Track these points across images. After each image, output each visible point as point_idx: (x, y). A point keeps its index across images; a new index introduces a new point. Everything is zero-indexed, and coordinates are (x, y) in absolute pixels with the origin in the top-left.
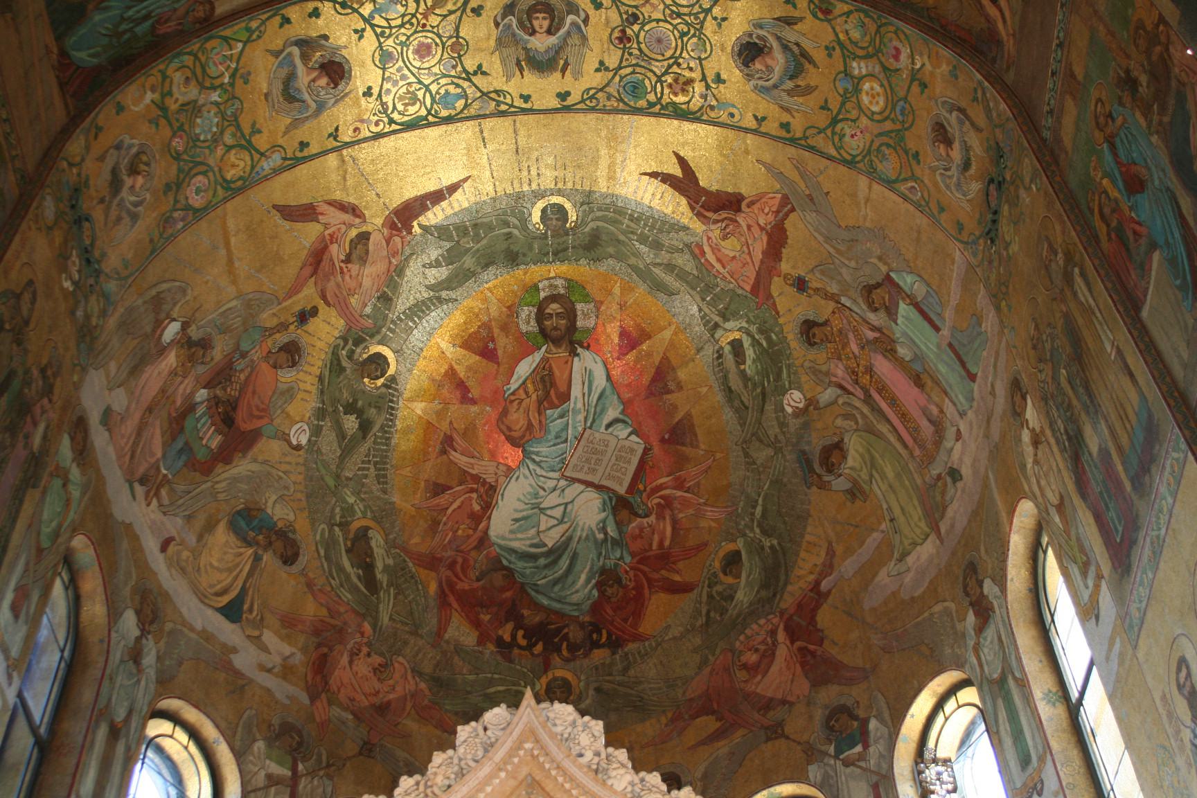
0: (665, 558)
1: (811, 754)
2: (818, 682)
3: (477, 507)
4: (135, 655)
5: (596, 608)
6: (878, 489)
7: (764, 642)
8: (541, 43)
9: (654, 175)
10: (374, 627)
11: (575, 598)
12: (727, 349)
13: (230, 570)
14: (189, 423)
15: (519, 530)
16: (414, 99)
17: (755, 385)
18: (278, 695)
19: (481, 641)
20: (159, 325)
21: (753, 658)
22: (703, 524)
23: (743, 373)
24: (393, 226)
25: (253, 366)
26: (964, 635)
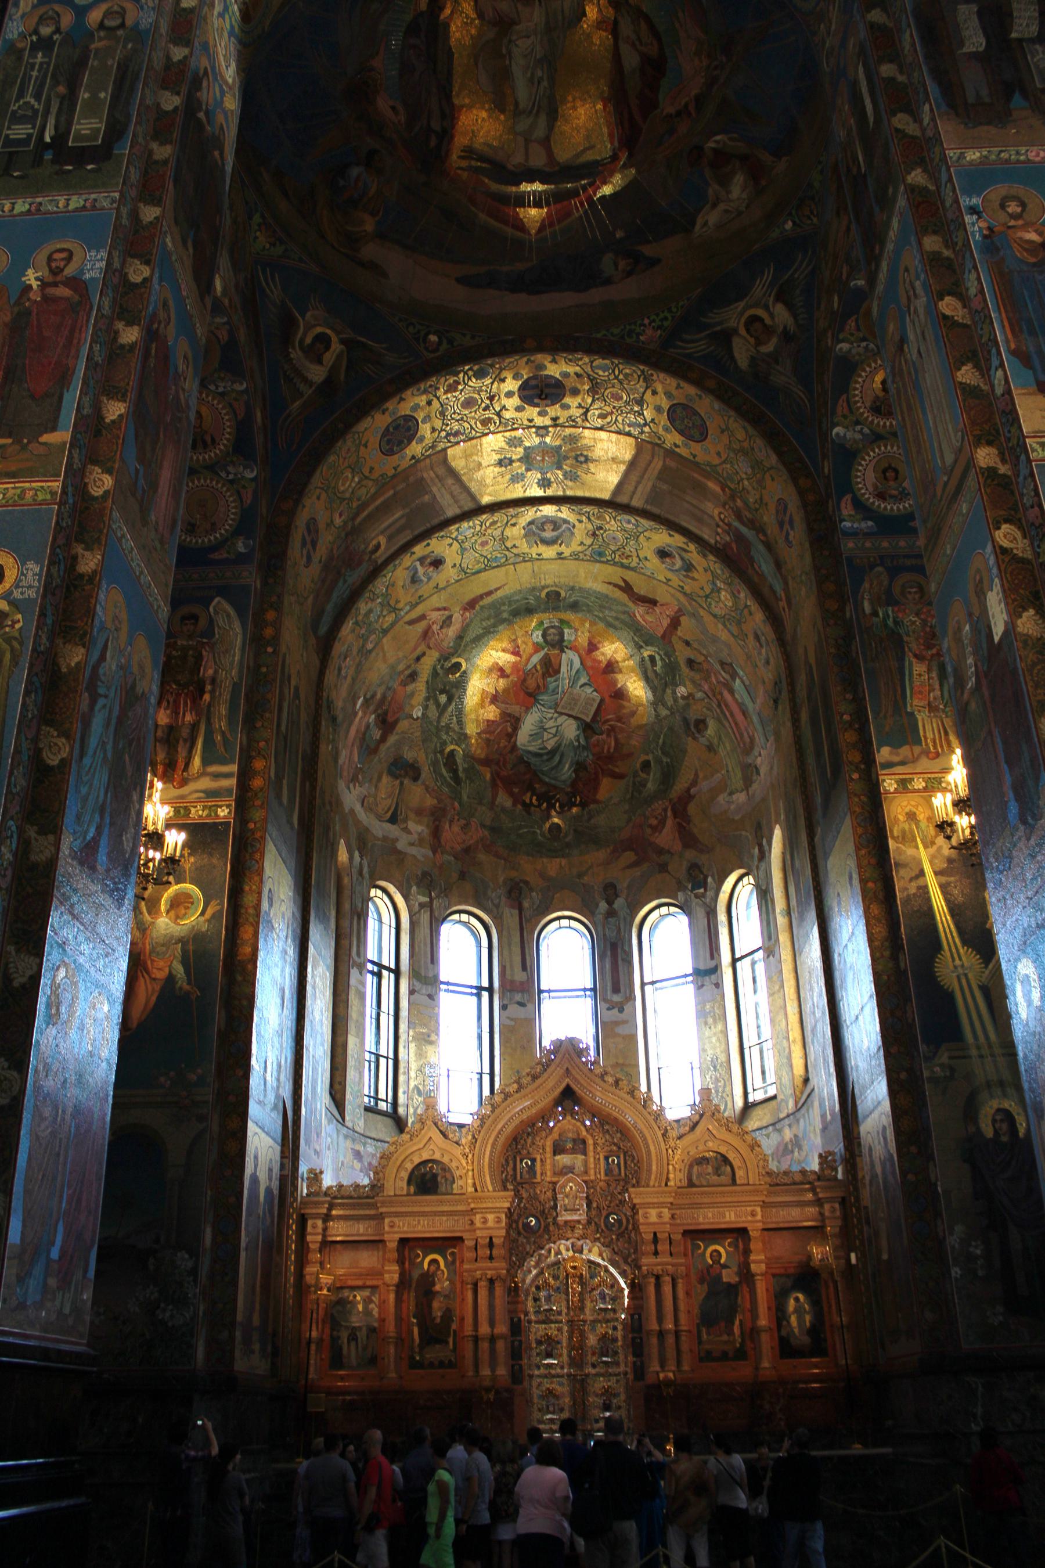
0: (610, 758)
1: (681, 887)
2: (686, 846)
3: (510, 730)
4: (360, 873)
5: (574, 784)
6: (722, 752)
7: (660, 814)
8: (548, 534)
9: (610, 583)
10: (460, 804)
11: (563, 778)
12: (647, 658)
13: (389, 796)
14: (367, 735)
15: (534, 740)
16: (479, 562)
17: (661, 679)
18: (419, 857)
19: (514, 804)
20: (355, 704)
21: (654, 822)
22: (633, 742)
23: (655, 672)
24: (465, 609)
25: (395, 691)
26: (753, 856)
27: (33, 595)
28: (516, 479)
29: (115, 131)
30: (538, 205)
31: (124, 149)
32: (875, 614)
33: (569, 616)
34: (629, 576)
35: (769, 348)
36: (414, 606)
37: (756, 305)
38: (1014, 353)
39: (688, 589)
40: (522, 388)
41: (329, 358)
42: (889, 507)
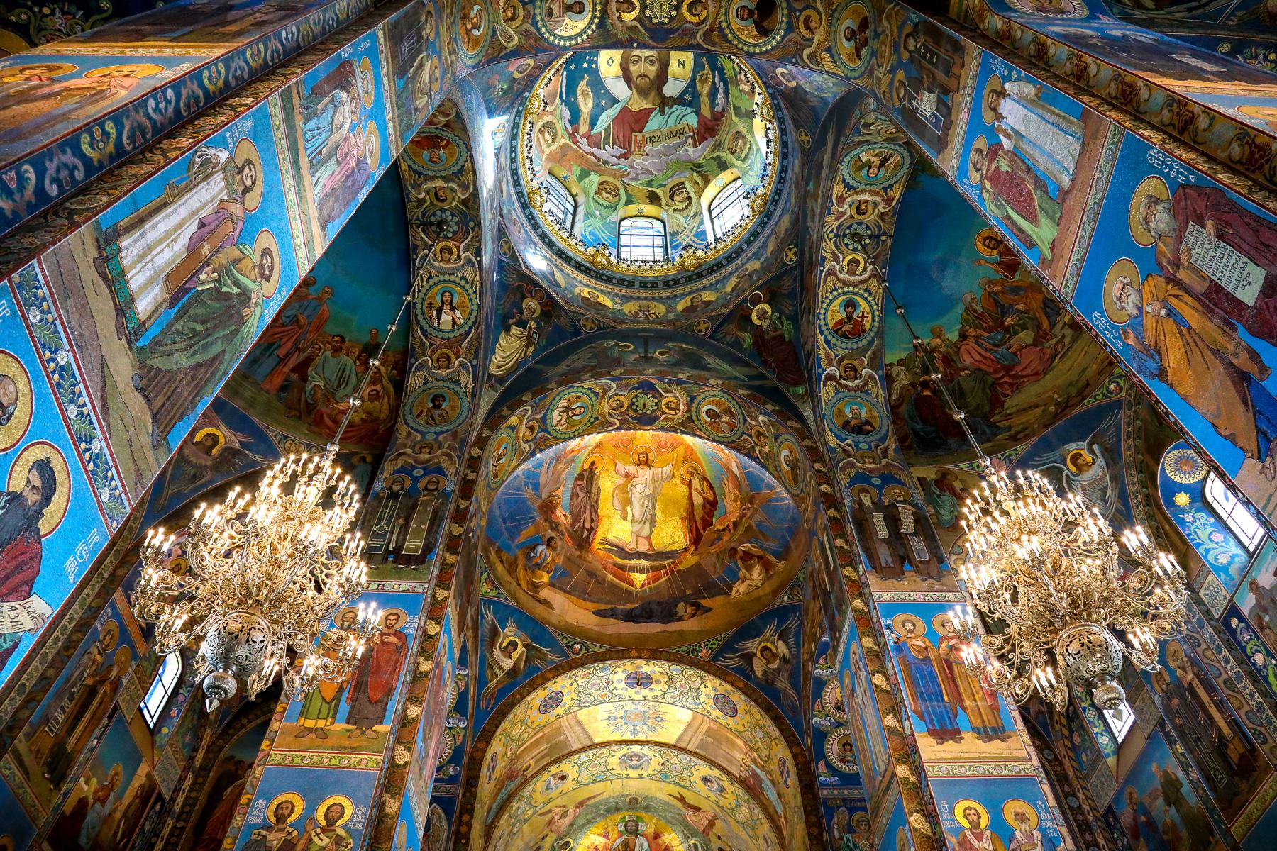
8: (634, 763)
27: (360, 826)
28: (617, 728)
29: (429, 548)
30: (642, 571)
31: (434, 561)
32: (841, 838)
33: (643, 814)
34: (684, 792)
35: (774, 666)
36: (545, 804)
37: (767, 641)
38: (915, 712)
39: (721, 803)
40: (629, 677)
41: (515, 655)
42: (848, 768)
